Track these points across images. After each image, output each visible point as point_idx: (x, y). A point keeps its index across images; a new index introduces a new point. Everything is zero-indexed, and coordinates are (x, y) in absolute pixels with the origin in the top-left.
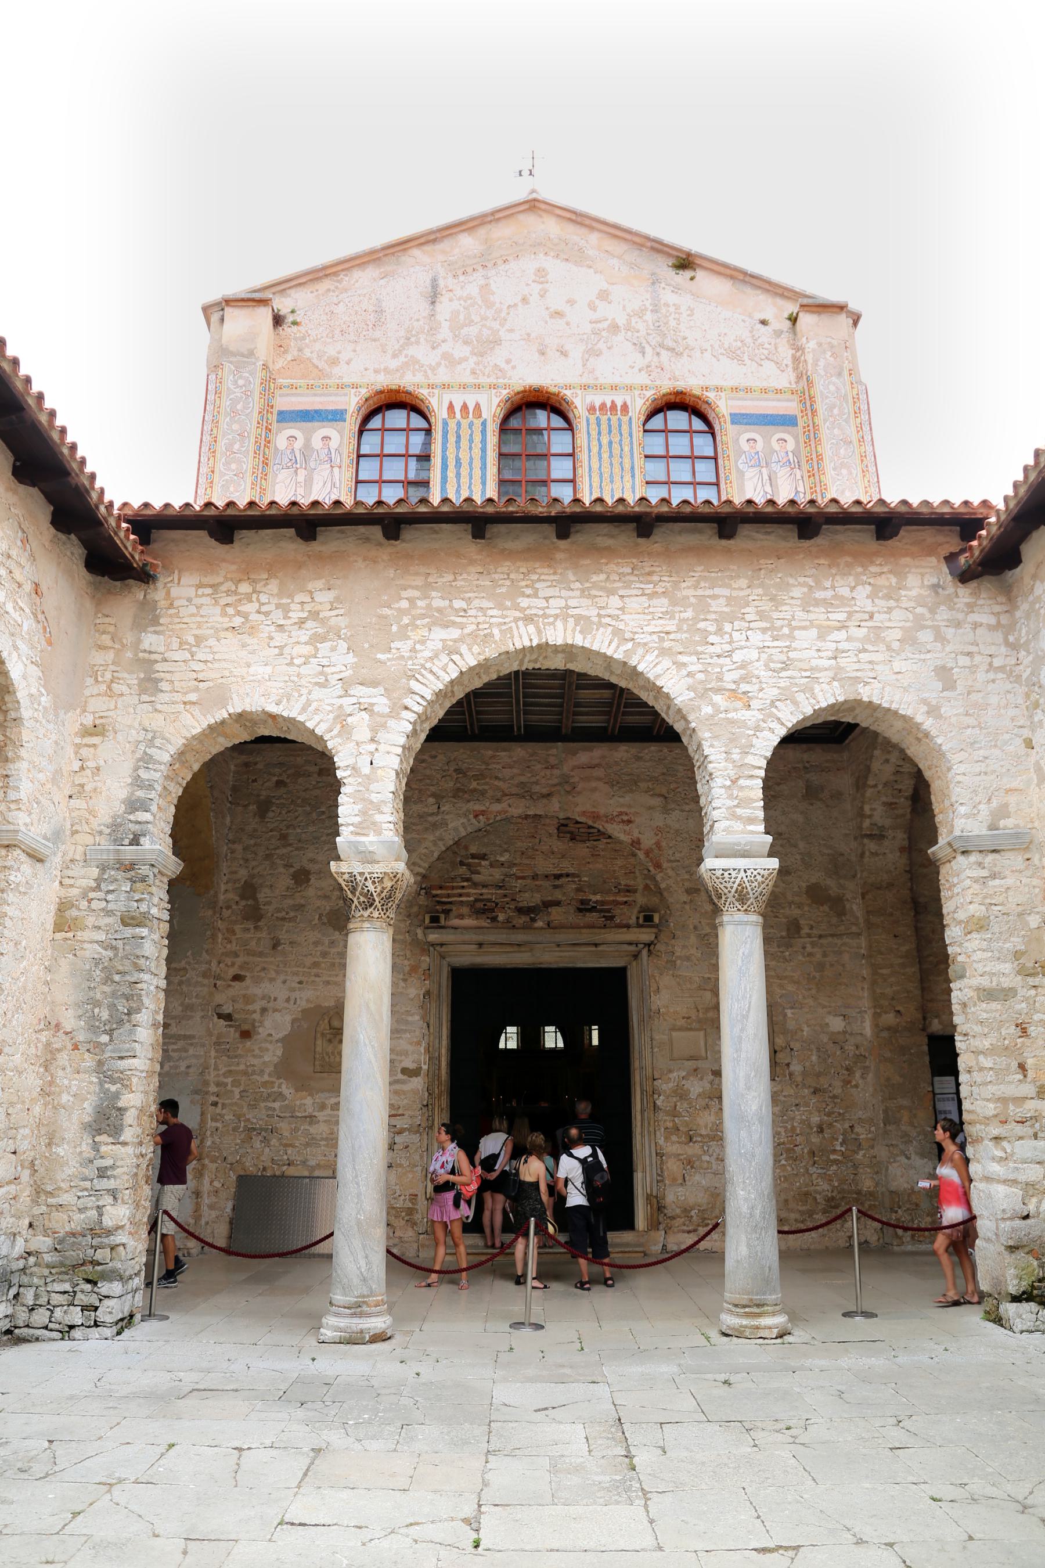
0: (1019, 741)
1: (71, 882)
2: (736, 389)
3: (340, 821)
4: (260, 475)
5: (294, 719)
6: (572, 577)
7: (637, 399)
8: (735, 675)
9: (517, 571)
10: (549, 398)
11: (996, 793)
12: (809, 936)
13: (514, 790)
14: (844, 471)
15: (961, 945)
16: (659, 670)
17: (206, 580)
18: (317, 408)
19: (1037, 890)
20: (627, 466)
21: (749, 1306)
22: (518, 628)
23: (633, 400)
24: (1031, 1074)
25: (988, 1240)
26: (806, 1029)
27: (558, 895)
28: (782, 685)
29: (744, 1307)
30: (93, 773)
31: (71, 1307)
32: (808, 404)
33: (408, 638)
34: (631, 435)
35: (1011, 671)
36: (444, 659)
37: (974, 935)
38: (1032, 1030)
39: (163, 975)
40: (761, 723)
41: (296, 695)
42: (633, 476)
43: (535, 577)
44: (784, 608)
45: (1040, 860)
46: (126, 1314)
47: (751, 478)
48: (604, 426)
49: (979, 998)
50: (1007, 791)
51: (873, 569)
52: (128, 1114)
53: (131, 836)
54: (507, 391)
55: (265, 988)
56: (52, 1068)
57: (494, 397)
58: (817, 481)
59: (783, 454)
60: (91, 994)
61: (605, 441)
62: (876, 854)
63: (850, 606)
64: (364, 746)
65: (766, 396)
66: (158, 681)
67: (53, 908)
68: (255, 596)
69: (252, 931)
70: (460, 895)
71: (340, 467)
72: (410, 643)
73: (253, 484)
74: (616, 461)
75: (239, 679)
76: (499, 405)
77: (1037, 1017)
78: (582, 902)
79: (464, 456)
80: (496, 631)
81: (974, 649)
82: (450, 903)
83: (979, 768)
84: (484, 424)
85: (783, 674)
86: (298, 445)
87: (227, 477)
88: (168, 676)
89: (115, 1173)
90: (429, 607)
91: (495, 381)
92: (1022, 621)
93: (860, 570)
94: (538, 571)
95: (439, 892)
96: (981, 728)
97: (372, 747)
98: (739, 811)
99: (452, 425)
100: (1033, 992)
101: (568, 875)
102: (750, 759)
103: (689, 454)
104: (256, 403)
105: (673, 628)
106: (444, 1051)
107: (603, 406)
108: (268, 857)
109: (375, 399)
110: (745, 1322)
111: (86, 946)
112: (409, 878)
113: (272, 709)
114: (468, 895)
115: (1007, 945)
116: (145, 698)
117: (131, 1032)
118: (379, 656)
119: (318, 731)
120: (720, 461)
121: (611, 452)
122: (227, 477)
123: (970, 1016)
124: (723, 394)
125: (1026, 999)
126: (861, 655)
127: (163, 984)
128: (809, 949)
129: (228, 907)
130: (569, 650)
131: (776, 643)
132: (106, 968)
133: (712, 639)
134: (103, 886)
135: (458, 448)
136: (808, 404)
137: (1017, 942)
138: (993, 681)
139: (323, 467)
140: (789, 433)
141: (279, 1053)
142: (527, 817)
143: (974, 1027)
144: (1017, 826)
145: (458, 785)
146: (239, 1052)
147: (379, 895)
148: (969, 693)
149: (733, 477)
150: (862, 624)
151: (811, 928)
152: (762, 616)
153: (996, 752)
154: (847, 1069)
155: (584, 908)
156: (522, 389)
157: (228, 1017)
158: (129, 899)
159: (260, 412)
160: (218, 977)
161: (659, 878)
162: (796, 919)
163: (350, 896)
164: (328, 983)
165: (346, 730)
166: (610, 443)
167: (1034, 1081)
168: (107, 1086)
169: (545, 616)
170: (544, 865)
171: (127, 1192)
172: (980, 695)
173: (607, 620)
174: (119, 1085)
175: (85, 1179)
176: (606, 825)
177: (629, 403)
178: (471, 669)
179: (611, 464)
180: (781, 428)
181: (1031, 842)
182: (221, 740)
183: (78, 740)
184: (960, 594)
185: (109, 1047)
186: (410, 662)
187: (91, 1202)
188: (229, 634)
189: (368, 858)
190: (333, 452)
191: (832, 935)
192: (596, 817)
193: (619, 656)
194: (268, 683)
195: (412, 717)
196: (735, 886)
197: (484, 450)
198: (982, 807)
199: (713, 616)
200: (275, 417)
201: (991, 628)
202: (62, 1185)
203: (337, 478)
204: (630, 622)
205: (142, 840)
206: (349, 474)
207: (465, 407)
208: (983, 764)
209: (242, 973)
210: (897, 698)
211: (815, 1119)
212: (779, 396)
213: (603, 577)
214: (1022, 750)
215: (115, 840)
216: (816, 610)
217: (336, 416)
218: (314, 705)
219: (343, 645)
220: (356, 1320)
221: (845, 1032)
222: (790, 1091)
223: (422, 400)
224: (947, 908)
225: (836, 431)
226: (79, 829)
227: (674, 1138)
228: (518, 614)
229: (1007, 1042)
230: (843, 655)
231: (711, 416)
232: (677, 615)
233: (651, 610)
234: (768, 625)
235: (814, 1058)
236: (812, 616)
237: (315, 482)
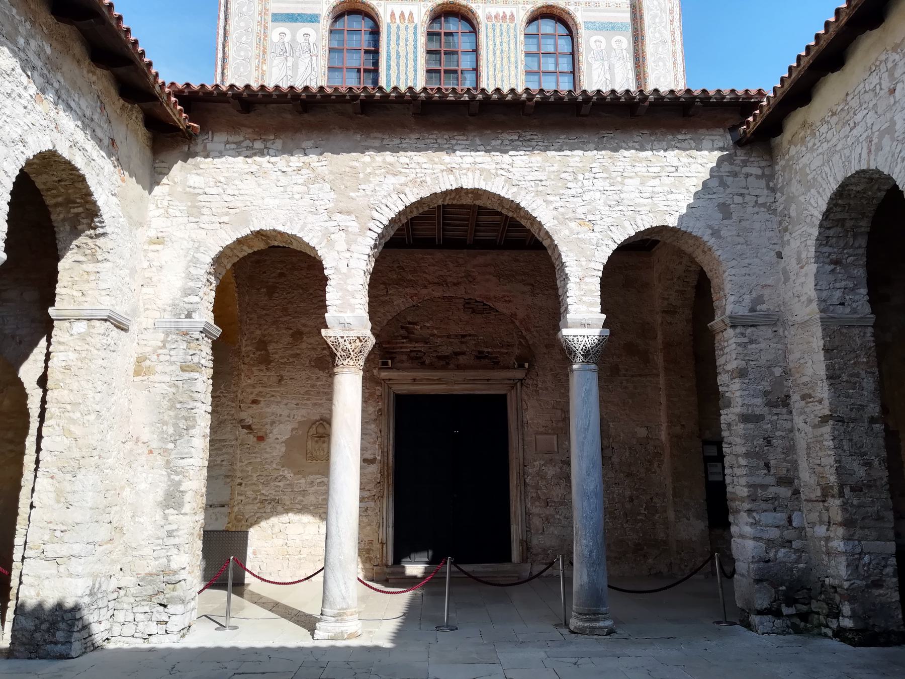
0: (773, 253)
1: (145, 342)
3: (327, 303)
4: (261, 61)
5: (295, 235)
6: (478, 141)
7: (521, 11)
8: (584, 209)
9: (442, 138)
10: (460, 9)
11: (756, 288)
12: (625, 375)
13: (436, 280)
14: (661, 64)
15: (728, 386)
16: (534, 206)
17: (231, 139)
19: (780, 352)
20: (513, 60)
21: (588, 614)
22: (443, 176)
23: (518, 12)
24: (773, 470)
25: (743, 575)
26: (622, 435)
27: (464, 348)
28: (615, 216)
29: (586, 615)
30: (157, 269)
31: (150, 622)
33: (370, 182)
34: (516, 38)
35: (770, 207)
36: (395, 197)
37: (737, 380)
38: (774, 442)
39: (210, 403)
40: (601, 241)
41: (296, 219)
43: (454, 142)
44: (619, 164)
45: (784, 332)
46: (187, 625)
48: (498, 30)
49: (739, 421)
50: (763, 287)
51: (680, 137)
52: (187, 494)
53: (186, 313)
54: (432, 3)
55: (274, 408)
56: (134, 466)
57: (422, 8)
60: (161, 416)
61: (498, 41)
62: (671, 323)
63: (663, 162)
64: (343, 254)
65: (609, 8)
66: (199, 208)
67: (133, 360)
68: (266, 151)
69: (265, 370)
70: (401, 348)
72: (372, 185)
73: (256, 67)
74: (505, 55)
75: (257, 208)
76: (425, 14)
77: (777, 434)
78: (480, 352)
80: (428, 179)
81: (746, 191)
82: (395, 353)
83: (744, 271)
84: (415, 27)
85: (617, 208)
86: (287, 39)
88: (207, 204)
89: (178, 534)
90: (384, 161)
92: (780, 172)
93: (670, 137)
94: (456, 137)
95: (387, 346)
96: (747, 245)
97: (348, 255)
98: (584, 299)
99: (394, 29)
100: (775, 418)
101: (470, 335)
102: (592, 265)
105: (544, 178)
106: (391, 447)
107: (497, 16)
108: (275, 323)
109: (340, 7)
110: (586, 625)
111: (156, 385)
112: (372, 341)
113: (280, 228)
114: (406, 348)
115: (760, 387)
116: (192, 219)
117: (188, 441)
118: (352, 194)
119: (312, 244)
122: (238, 61)
123: (733, 432)
125: (771, 422)
126: (669, 196)
127: (210, 409)
128: (625, 383)
129: (248, 356)
130: (477, 193)
131: (612, 188)
132: (170, 399)
133: (570, 185)
134: (167, 345)
135: (398, 44)
137: (765, 385)
138: (757, 213)
140: (624, 36)
141: (283, 449)
142: (444, 298)
143: (736, 439)
144: (769, 309)
145: (399, 277)
146: (257, 450)
147: (353, 351)
148: (740, 221)
150: (671, 174)
151: (627, 370)
152: (605, 169)
153: (756, 260)
154: (649, 462)
155: (480, 356)
157: (249, 427)
158: (186, 354)
159: (259, 14)
160: (242, 401)
161: (528, 338)
162: (617, 365)
163: (335, 352)
164: (315, 404)
165: (330, 243)
166: (502, 42)
167: (774, 475)
168: (172, 477)
169: (460, 169)
170: (455, 329)
171: (187, 545)
172: (748, 222)
173: (502, 172)
174: (181, 476)
175: (158, 538)
176: (494, 303)
178: (412, 204)
179: (502, 59)
181: (778, 320)
182: (245, 248)
183: (146, 247)
184: (739, 153)
185: (174, 452)
186: (372, 199)
187: (163, 553)
188: (249, 177)
189: (345, 326)
190: (312, 45)
191: (640, 376)
192: (489, 299)
193: (509, 196)
194: (277, 211)
195: (375, 236)
196: (582, 346)
197: (415, 47)
198: (745, 297)
199: (570, 170)
200: (269, 18)
201: (758, 177)
202: (143, 542)
204: (516, 174)
205: (194, 315)
207: (402, 15)
208: (748, 269)
209: (259, 399)
210: (691, 225)
211: (628, 493)
213: (499, 142)
214: (775, 259)
215: (175, 315)
216: (640, 165)
217: (313, 19)
218: (310, 226)
219: (327, 186)
220: (338, 624)
221: (647, 438)
222: (611, 474)
223: (373, 9)
224: (720, 361)
226: (149, 307)
227: (537, 503)
228: (443, 167)
229: (757, 449)
230: (657, 195)
231: (571, 24)
232: (547, 168)
233: (531, 165)
234: (608, 176)
235: (627, 454)
236: (637, 169)
237: (300, 67)
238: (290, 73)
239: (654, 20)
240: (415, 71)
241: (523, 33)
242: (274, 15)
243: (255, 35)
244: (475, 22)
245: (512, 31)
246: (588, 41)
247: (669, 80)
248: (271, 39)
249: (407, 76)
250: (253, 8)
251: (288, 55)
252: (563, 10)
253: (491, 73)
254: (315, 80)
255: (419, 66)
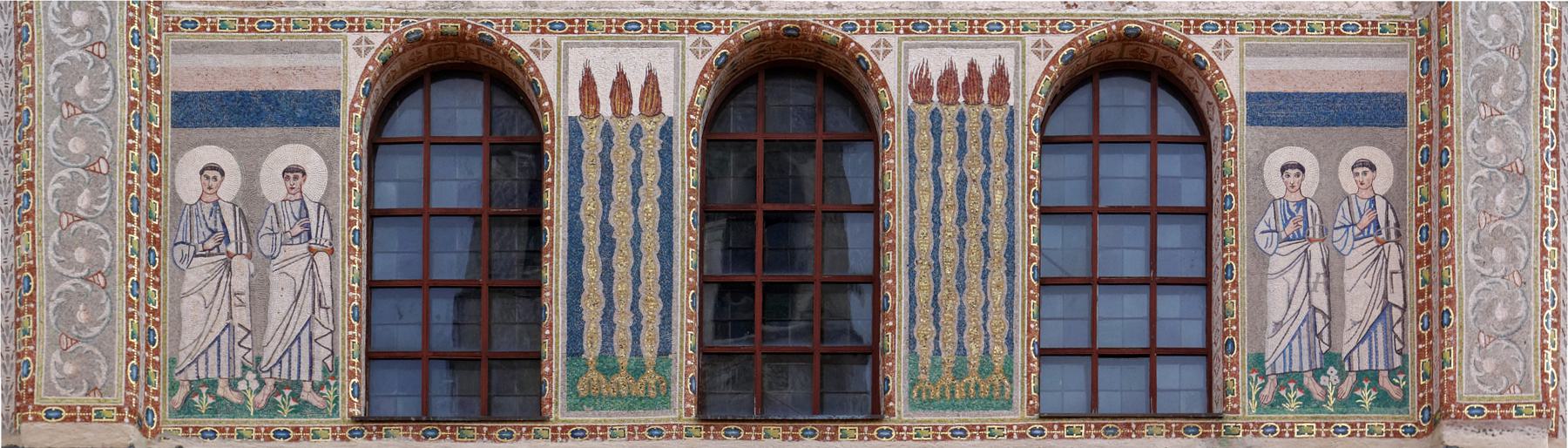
2: (1267, 24)
7: (1031, 58)
14: (1499, 254)
18: (267, 87)
20: (998, 244)
23: (1021, 62)
32: (1435, 67)
34: (1010, 159)
42: (1011, 273)
47: (1284, 271)
48: (949, 138)
57: (690, 57)
58: (1436, 277)
59: (1363, 204)
61: (949, 177)
65: (1337, 41)
71: (331, 252)
74: (973, 229)
76: (701, 80)
79: (621, 221)
84: (667, 132)
86: (229, 189)
87: (67, 285)
91: (692, 10)
99: (592, 139)
103: (1142, 200)
104: (123, 79)
107: (949, 74)
109: (406, 57)
120: (1216, 222)
121: (962, 208)
122: (67, 285)
124: (1233, 40)
135: (606, 199)
136: (1435, 67)
139: (291, 251)
140: (1382, 145)
149: (1242, 270)
156: (754, 31)
166: (962, 182)
177: (1010, 70)
179: (962, 241)
180: (1366, 131)
190: (312, 208)
197: (666, 204)
203: (326, 280)
206: (353, 269)
207: (621, 84)
212: (1368, 41)
223: (518, 64)
225: (1493, 145)
231: (1204, 98)
237: (275, 292)
238: (242, 316)
239: (1487, 88)
240: (667, 295)
241: (1036, 143)
242: (180, 99)
243: (121, 182)
244: (872, 102)
245: (998, 137)
246: (1260, 167)
247: (1521, 312)
248: (174, 193)
249: (638, 317)
250: (109, 85)
251: (232, 248)
252: (1176, 49)
253: (924, 296)
254: (327, 341)
255: (677, 279)
